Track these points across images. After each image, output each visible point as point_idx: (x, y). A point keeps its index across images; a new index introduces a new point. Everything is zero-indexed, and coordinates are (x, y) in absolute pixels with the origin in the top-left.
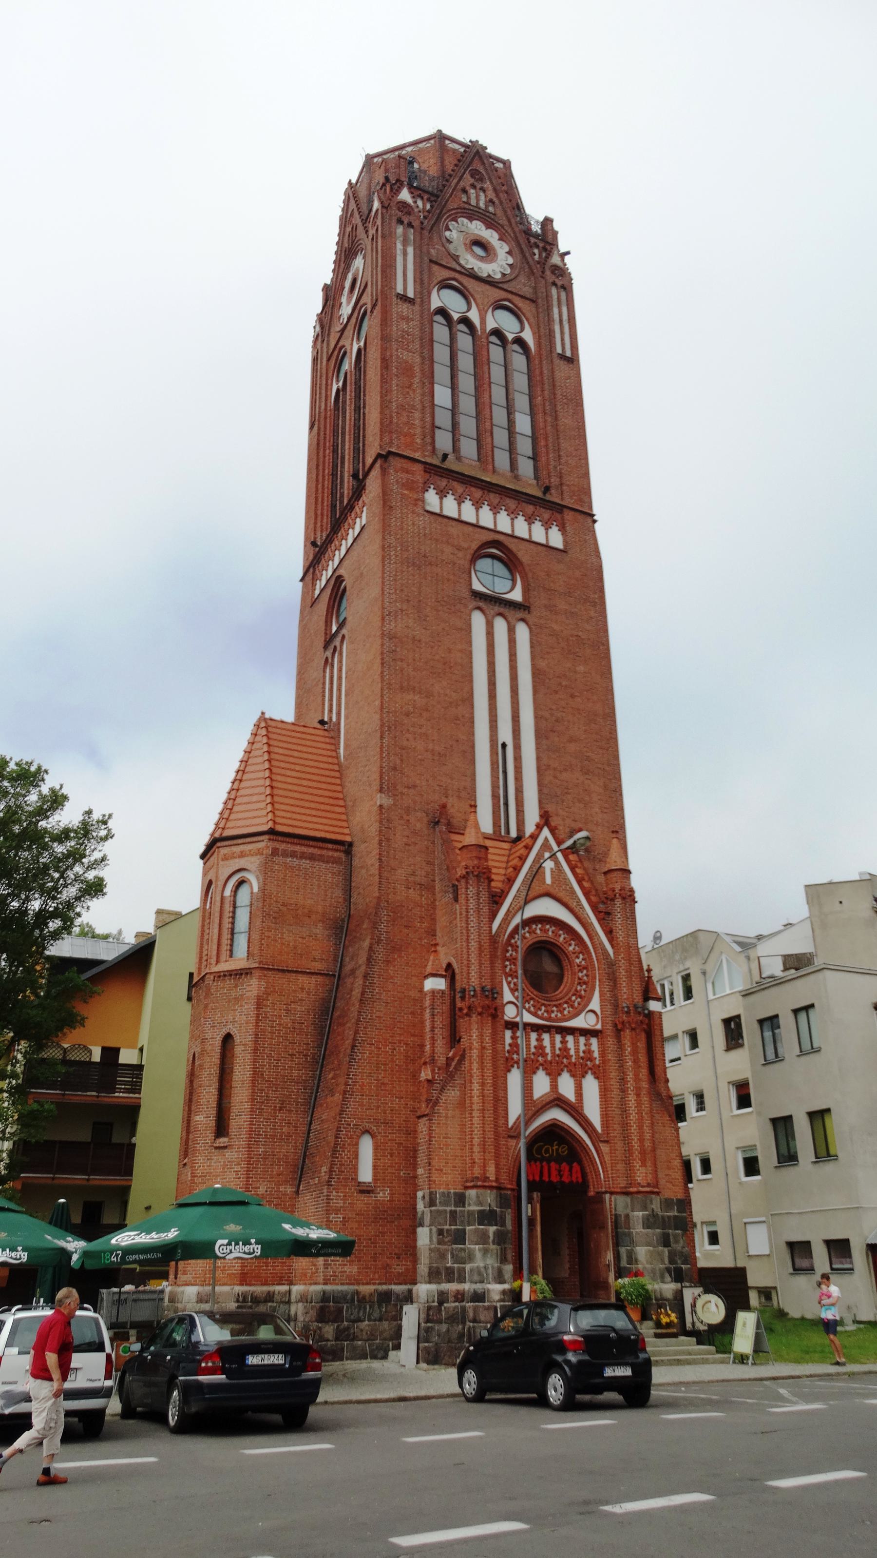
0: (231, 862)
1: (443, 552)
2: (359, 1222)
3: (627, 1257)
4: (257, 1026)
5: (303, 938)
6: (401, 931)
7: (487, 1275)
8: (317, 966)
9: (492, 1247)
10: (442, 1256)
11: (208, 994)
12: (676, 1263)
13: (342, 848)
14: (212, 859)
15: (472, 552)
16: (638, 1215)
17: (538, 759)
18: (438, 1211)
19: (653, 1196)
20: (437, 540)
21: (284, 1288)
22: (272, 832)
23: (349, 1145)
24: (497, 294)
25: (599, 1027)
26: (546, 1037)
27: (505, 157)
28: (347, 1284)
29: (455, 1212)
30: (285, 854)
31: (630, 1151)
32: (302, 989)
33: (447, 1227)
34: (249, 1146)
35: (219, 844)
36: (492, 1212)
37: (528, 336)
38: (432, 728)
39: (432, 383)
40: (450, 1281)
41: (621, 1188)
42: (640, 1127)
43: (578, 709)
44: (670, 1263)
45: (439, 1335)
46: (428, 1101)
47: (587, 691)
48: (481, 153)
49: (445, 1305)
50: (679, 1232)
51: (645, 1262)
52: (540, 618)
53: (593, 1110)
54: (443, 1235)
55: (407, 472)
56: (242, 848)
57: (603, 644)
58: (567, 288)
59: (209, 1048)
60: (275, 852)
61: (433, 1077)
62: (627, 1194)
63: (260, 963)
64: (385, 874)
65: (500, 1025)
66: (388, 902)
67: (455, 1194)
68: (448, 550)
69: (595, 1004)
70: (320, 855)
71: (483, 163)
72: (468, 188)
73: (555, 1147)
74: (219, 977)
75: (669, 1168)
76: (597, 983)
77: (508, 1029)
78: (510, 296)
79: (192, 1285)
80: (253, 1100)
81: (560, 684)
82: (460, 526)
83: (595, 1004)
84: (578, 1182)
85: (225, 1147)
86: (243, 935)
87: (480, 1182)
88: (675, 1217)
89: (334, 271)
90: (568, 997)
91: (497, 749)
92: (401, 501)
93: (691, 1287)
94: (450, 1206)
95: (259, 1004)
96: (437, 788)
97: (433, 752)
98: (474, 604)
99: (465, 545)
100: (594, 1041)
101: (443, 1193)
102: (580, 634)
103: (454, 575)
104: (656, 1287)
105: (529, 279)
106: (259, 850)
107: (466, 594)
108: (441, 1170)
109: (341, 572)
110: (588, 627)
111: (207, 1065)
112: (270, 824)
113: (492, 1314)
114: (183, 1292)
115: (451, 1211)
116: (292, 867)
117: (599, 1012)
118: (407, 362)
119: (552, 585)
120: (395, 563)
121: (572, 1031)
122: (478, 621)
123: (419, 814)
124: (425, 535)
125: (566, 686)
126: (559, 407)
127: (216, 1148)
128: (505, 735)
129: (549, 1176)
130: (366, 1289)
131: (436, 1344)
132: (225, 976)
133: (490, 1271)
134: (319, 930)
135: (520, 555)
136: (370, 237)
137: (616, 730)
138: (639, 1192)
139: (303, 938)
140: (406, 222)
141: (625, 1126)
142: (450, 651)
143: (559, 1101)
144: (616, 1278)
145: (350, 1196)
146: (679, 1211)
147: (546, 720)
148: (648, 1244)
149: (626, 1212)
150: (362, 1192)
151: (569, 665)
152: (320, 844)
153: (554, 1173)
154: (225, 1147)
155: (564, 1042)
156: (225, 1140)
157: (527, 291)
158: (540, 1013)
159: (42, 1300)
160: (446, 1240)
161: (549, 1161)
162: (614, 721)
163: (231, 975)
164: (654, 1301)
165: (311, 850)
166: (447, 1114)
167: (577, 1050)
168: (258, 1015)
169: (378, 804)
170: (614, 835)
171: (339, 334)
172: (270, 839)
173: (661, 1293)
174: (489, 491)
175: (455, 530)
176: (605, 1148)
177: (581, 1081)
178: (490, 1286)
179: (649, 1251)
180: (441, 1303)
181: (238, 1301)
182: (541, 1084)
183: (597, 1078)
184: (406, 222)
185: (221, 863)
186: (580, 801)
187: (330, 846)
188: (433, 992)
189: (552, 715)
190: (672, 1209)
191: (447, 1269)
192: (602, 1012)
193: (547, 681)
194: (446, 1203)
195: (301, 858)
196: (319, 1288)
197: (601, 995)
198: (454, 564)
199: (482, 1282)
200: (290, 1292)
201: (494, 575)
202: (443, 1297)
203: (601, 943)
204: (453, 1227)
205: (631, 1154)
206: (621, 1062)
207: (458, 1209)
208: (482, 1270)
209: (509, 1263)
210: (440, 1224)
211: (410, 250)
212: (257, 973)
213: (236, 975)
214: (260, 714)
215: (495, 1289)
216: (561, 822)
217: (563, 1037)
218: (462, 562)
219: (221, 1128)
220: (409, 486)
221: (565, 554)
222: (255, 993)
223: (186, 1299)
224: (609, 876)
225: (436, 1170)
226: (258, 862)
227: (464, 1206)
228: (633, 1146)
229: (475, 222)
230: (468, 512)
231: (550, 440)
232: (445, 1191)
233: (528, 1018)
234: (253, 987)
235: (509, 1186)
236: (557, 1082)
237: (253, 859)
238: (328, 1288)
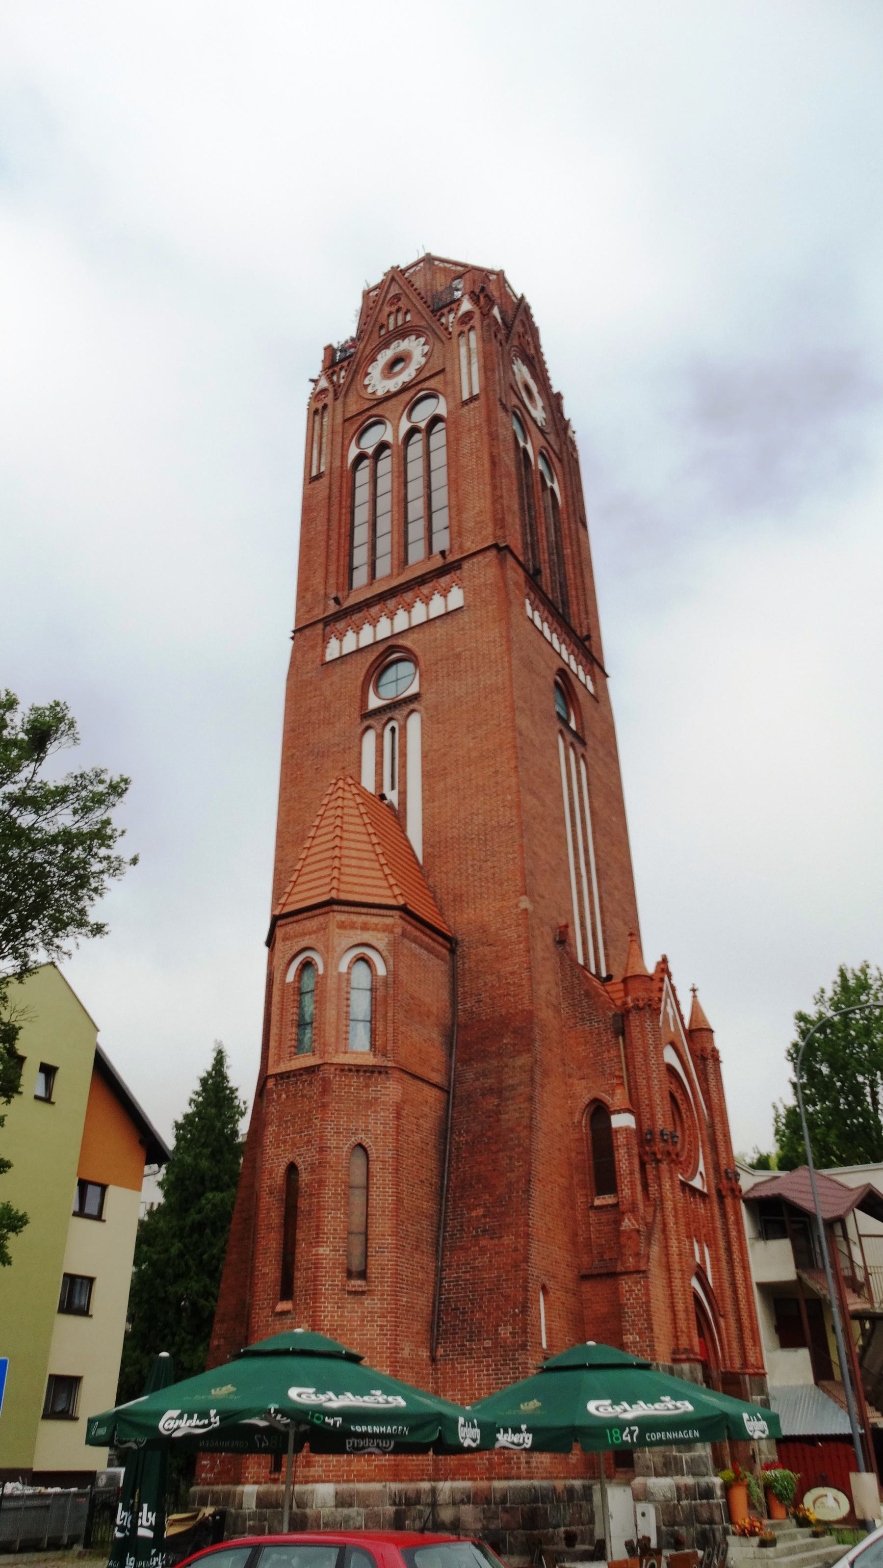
0: (352, 932)
8: (436, 1078)
11: (326, 1089)
13: (448, 945)
14: (305, 922)
21: (425, 1485)
22: (403, 909)
28: (546, 1478)
32: (427, 1102)
34: (395, 1293)
35: (336, 907)
46: (637, 1255)
56: (363, 918)
59: (331, 1158)
60: (404, 934)
63: (397, 1062)
64: (534, 987)
74: (342, 1070)
76: (700, 1144)
79: (323, 1481)
80: (395, 1234)
82: (549, 646)
85: (363, 1293)
86: (361, 1024)
89: (544, 363)
106: (387, 926)
111: (330, 1182)
112: (401, 901)
114: (312, 1492)
116: (415, 955)
123: (547, 929)
127: (350, 1293)
130: (560, 1484)
132: (350, 1070)
134: (435, 1035)
152: (435, 936)
154: (363, 1293)
156: (359, 1282)
159: (145, 1506)
163: (358, 1071)
165: (426, 939)
169: (523, 906)
171: (372, 403)
172: (401, 917)
181: (394, 1504)
185: (337, 930)
187: (441, 940)
188: (627, 1129)
195: (421, 946)
196: (524, 1483)
200: (434, 1491)
212: (397, 1074)
213: (365, 1072)
223: (318, 1500)
224: (697, 1034)
226: (386, 940)
234: (391, 1090)
237: (380, 935)
238: (536, 1483)
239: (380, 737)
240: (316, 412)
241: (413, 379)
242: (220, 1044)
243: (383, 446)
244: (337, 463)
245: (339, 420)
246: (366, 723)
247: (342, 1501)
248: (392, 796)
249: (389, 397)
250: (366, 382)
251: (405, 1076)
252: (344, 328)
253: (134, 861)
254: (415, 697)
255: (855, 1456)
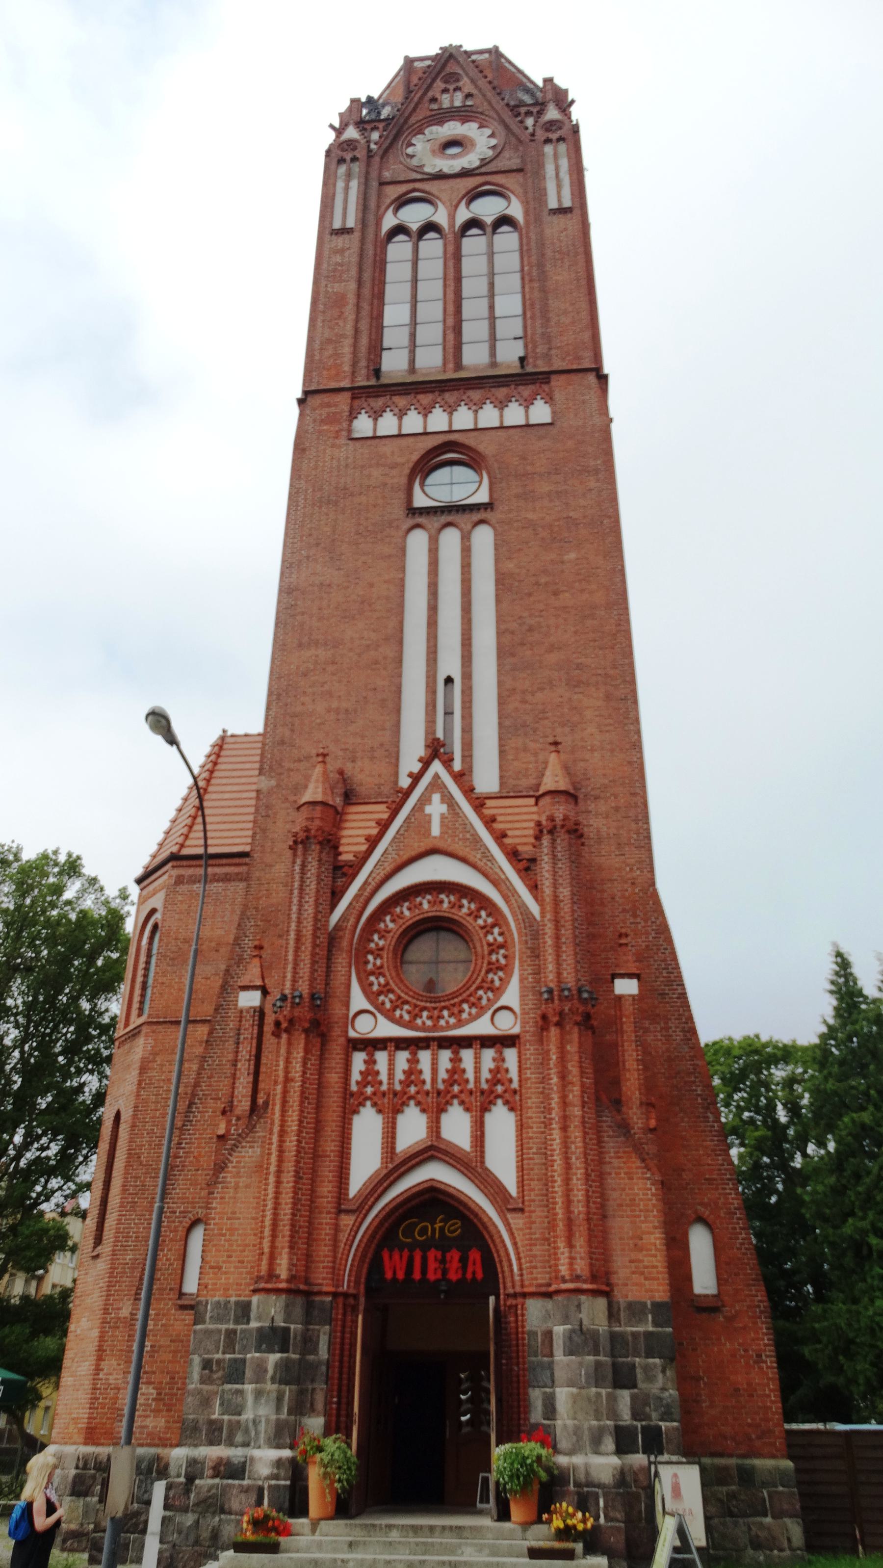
1: (369, 476)
2: (175, 1352)
3: (545, 1405)
4: (138, 1095)
5: (207, 978)
6: (273, 944)
7: (257, 1433)
9: (271, 1387)
10: (206, 1402)
12: (648, 1418)
15: (411, 465)
16: (559, 1330)
17: (500, 684)
18: (208, 1332)
19: (583, 1298)
20: (362, 467)
23: (171, 1240)
24: (470, 183)
25: (516, 1030)
26: (425, 1057)
27: (489, 45)
29: (234, 1332)
30: (193, 880)
31: (552, 1226)
33: (219, 1356)
36: (273, 1329)
37: (516, 210)
38: (340, 682)
39: (382, 303)
40: (211, 1443)
41: (541, 1285)
42: (567, 1181)
43: (565, 607)
44: (635, 1416)
45: (180, 1532)
47: (580, 581)
48: (454, 52)
49: (197, 1482)
50: (657, 1361)
51: (565, 1416)
52: (510, 511)
53: (502, 1160)
54: (211, 1371)
55: (329, 405)
57: (610, 517)
58: (569, 136)
61: (228, 1130)
62: (548, 1295)
65: (336, 1049)
66: (256, 909)
67: (237, 1303)
68: (376, 473)
69: (512, 996)
70: (238, 874)
71: (458, 62)
72: (438, 96)
73: (437, 1226)
75: (638, 1248)
77: (356, 1049)
78: (489, 178)
81: (537, 584)
83: (512, 996)
84: (474, 1278)
87: (266, 1283)
88: (648, 1334)
90: (468, 992)
92: (318, 439)
93: (688, 1463)
94: (228, 1322)
95: (143, 1069)
96: (340, 753)
97: (337, 711)
98: (411, 522)
99: (400, 460)
100: (511, 1055)
101: (218, 1302)
102: (571, 514)
103: (384, 497)
104: (578, 1460)
105: (516, 149)
107: (399, 511)
108: (220, 1268)
110: (582, 502)
113: (253, 1499)
115: (227, 1330)
117: (517, 1009)
118: (335, 294)
119: (529, 468)
120: (305, 507)
121: (467, 1042)
122: (418, 542)
124: (347, 465)
125: (546, 584)
126: (548, 267)
128: (450, 664)
129: (424, 1271)
131: (174, 1546)
133: (262, 1427)
135: (481, 448)
137: (628, 621)
138: (558, 1292)
139: (207, 978)
140: (348, 158)
141: (547, 1182)
142: (371, 585)
143: (434, 1150)
144: (497, 1446)
145: (164, 1315)
146: (655, 1324)
147: (512, 633)
148: (571, 1384)
149: (544, 1327)
150: (183, 1307)
151: (553, 556)
153: (432, 1265)
155: (456, 1060)
157: (515, 163)
158: (419, 1021)
160: (215, 1376)
161: (425, 1247)
162: (626, 609)
164: (572, 1487)
166: (237, 1184)
167: (477, 1070)
168: (140, 1083)
170: (553, 748)
173: (587, 1473)
174: (443, 391)
175: (387, 448)
176: (517, 1221)
177: (482, 1117)
178: (256, 1453)
179: (572, 1394)
180: (190, 1479)
182: (412, 1128)
183: (512, 1109)
184: (348, 158)
186: (563, 725)
189: (520, 625)
190: (641, 1320)
191: (211, 1422)
192: (521, 1005)
193: (517, 584)
194: (219, 1319)
197: (522, 980)
198: (385, 484)
199: (246, 1445)
201: (452, 484)
202: (194, 1470)
203: (523, 907)
204: (228, 1356)
205: (556, 1226)
206: (544, 1079)
207: (239, 1327)
208: (251, 1424)
209: (318, 1415)
210: (208, 1352)
211: (354, 184)
214: (221, 733)
215: (265, 1458)
216: (532, 759)
217: (456, 1053)
218: (396, 480)
220: (331, 419)
221: (551, 428)
222: (139, 1056)
225: (211, 1267)
227: (248, 1323)
228: (556, 1214)
229: (446, 125)
230: (413, 422)
231: (537, 306)
232: (222, 1299)
233: (386, 1029)
235: (325, 1289)
236: (438, 1121)
242: (835, 944)
251: (160, 1028)
255: (488, 1413)
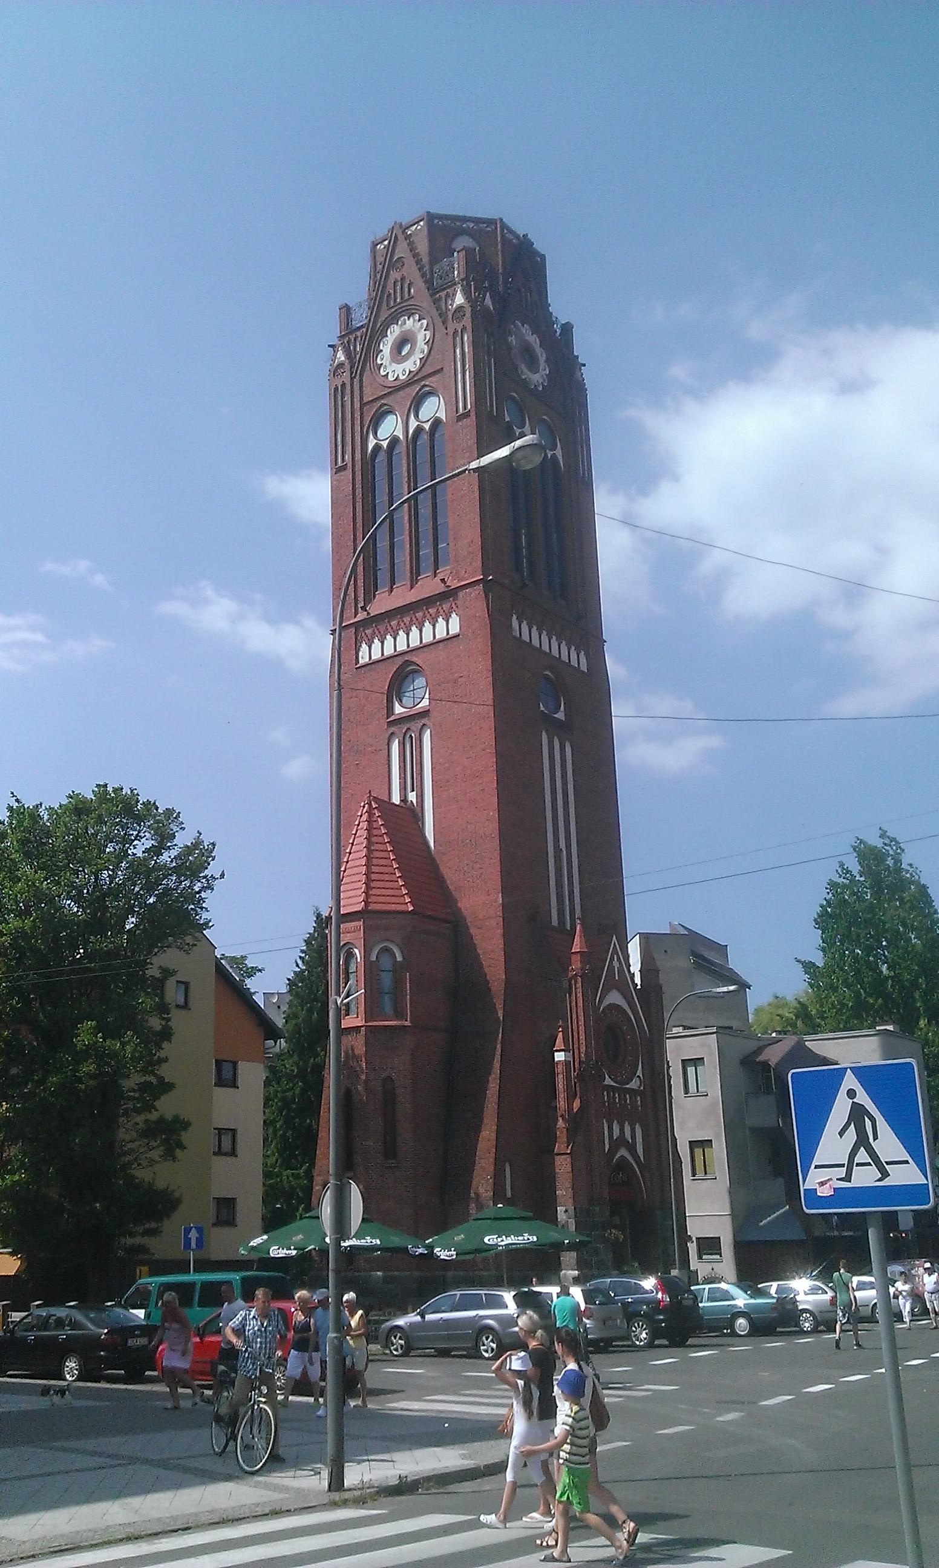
86: (386, 997)
91: (558, 850)
109: (414, 659)
127: (387, 1168)
136: (451, 331)
219: (390, 1150)
239: (402, 745)
240: (336, 389)
241: (420, 369)
243: (394, 441)
244: (358, 456)
245: (357, 405)
246: (392, 729)
247: (386, 1280)
248: (412, 797)
249: (401, 387)
250: (379, 362)
252: (357, 291)
253: (222, 876)
254: (425, 713)
